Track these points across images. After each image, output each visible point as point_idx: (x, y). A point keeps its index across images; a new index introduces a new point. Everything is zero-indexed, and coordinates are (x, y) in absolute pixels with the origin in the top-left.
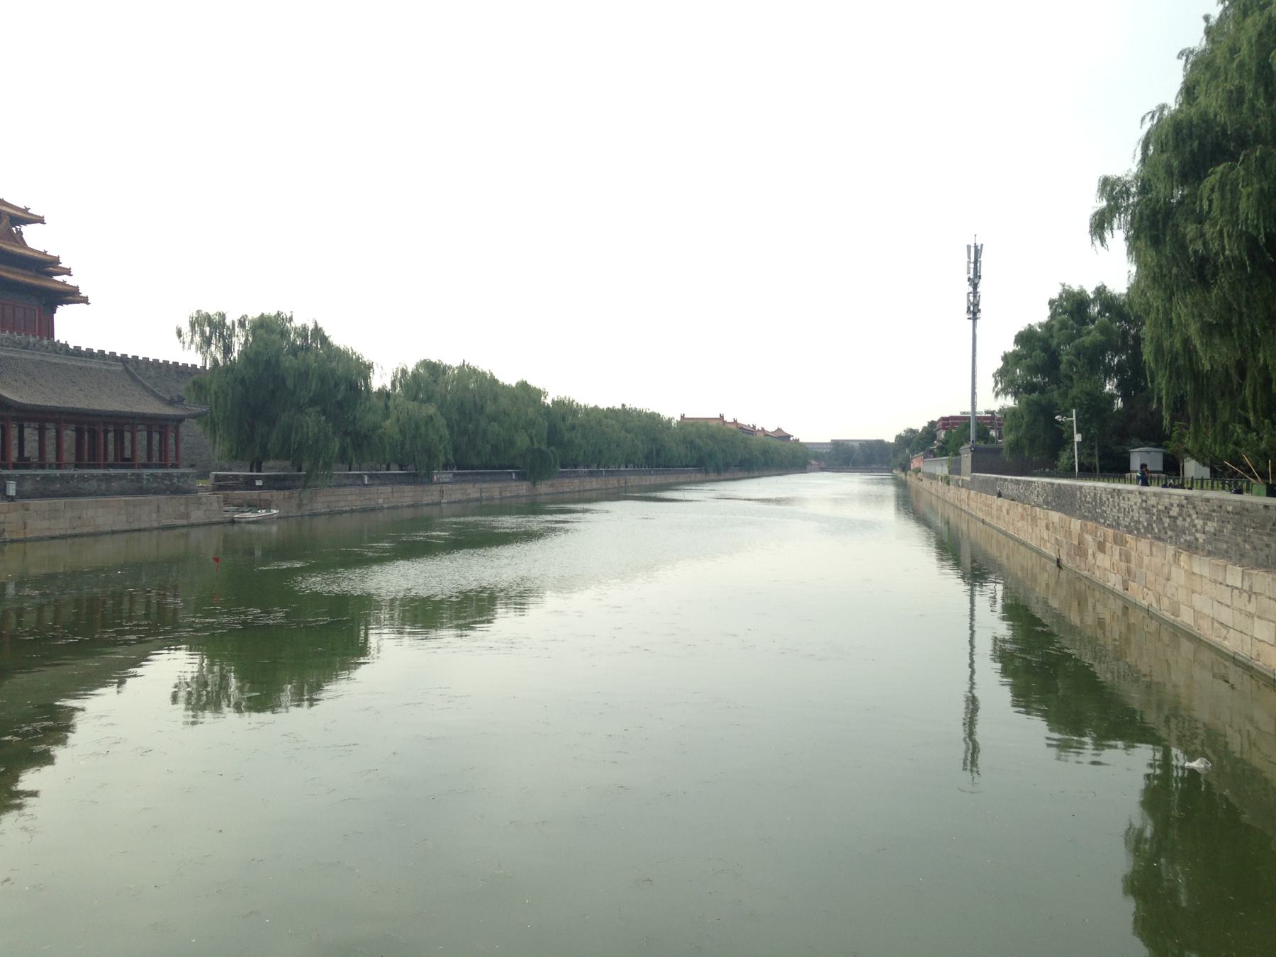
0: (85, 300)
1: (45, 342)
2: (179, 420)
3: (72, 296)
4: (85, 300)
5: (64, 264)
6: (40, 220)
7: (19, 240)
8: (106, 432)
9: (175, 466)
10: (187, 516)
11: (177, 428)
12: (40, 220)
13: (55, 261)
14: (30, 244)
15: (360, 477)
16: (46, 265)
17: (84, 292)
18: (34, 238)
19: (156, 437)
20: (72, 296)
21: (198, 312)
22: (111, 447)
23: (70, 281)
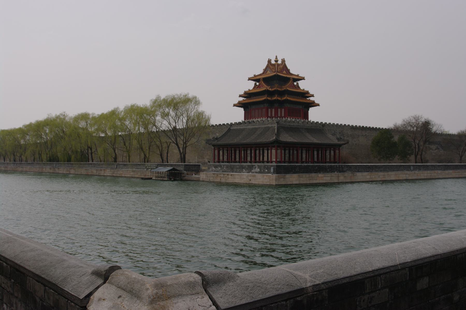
0: (318, 105)
1: (307, 121)
2: (340, 145)
3: (313, 104)
4: (318, 105)
5: (311, 93)
6: (303, 79)
7: (298, 87)
11: (339, 150)
12: (303, 79)
13: (308, 93)
14: (302, 88)
16: (305, 94)
17: (316, 102)
18: (303, 85)
19: (332, 152)
20: (313, 104)
22: (316, 156)
23: (312, 99)
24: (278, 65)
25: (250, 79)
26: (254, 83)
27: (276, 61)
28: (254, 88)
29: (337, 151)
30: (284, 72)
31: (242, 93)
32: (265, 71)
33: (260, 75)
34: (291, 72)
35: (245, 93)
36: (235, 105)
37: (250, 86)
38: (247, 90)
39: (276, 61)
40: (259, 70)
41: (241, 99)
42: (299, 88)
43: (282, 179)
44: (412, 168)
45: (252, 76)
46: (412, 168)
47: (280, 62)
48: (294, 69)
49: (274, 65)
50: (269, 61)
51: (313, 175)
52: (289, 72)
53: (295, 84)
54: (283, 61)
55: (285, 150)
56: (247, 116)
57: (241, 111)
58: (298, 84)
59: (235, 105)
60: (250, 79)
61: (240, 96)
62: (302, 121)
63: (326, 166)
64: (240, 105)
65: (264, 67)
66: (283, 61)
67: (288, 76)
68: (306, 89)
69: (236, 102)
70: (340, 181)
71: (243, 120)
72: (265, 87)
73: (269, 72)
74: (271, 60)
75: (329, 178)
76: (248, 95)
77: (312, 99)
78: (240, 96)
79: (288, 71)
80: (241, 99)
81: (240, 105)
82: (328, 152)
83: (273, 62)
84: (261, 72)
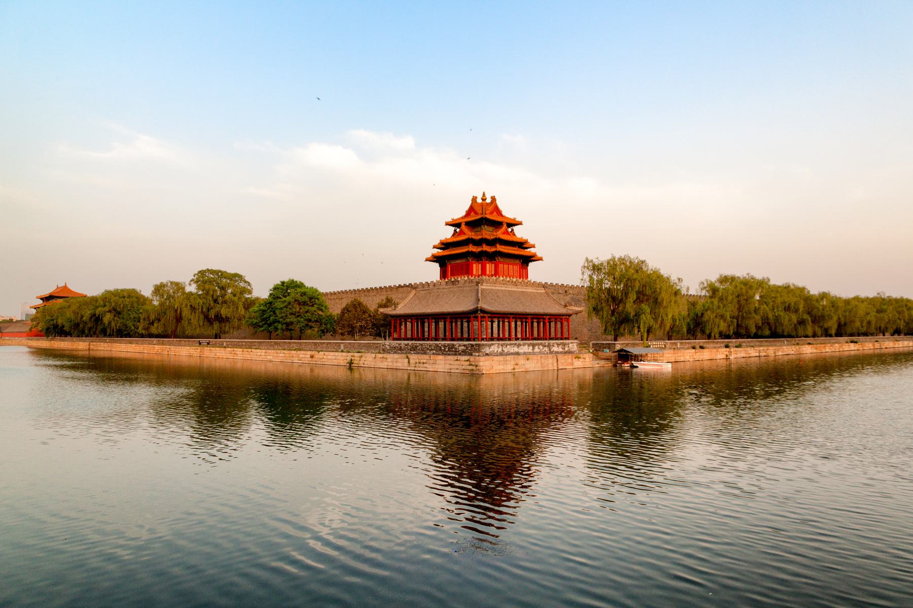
0: (541, 259)
2: (570, 315)
4: (541, 259)
5: (531, 241)
6: (520, 223)
8: (550, 323)
9: (568, 339)
10: (572, 364)
11: (568, 321)
12: (520, 223)
13: (526, 242)
15: (676, 344)
16: (522, 245)
17: (539, 255)
18: (520, 233)
21: (587, 259)
23: (532, 250)
24: (487, 204)
25: (447, 224)
26: (453, 228)
27: (484, 200)
28: (453, 235)
29: (565, 323)
31: (437, 242)
32: (468, 213)
33: (462, 218)
34: (504, 214)
35: (442, 243)
36: (427, 260)
37: (448, 233)
38: (443, 238)
39: (484, 200)
40: (459, 212)
41: (436, 251)
42: (514, 235)
45: (449, 220)
47: (489, 200)
48: (508, 211)
49: (482, 205)
50: (474, 199)
52: (502, 215)
53: (510, 230)
54: (493, 199)
55: (492, 322)
56: (443, 275)
57: (436, 266)
59: (427, 260)
60: (447, 224)
61: (435, 247)
64: (436, 259)
65: (467, 207)
66: (493, 199)
67: (499, 219)
68: (525, 238)
69: (429, 255)
71: (438, 279)
72: (469, 234)
73: (472, 214)
76: (445, 245)
77: (532, 250)
78: (435, 247)
79: (499, 213)
80: (436, 251)
81: (436, 259)
82: (553, 324)
83: (479, 201)
84: (464, 214)
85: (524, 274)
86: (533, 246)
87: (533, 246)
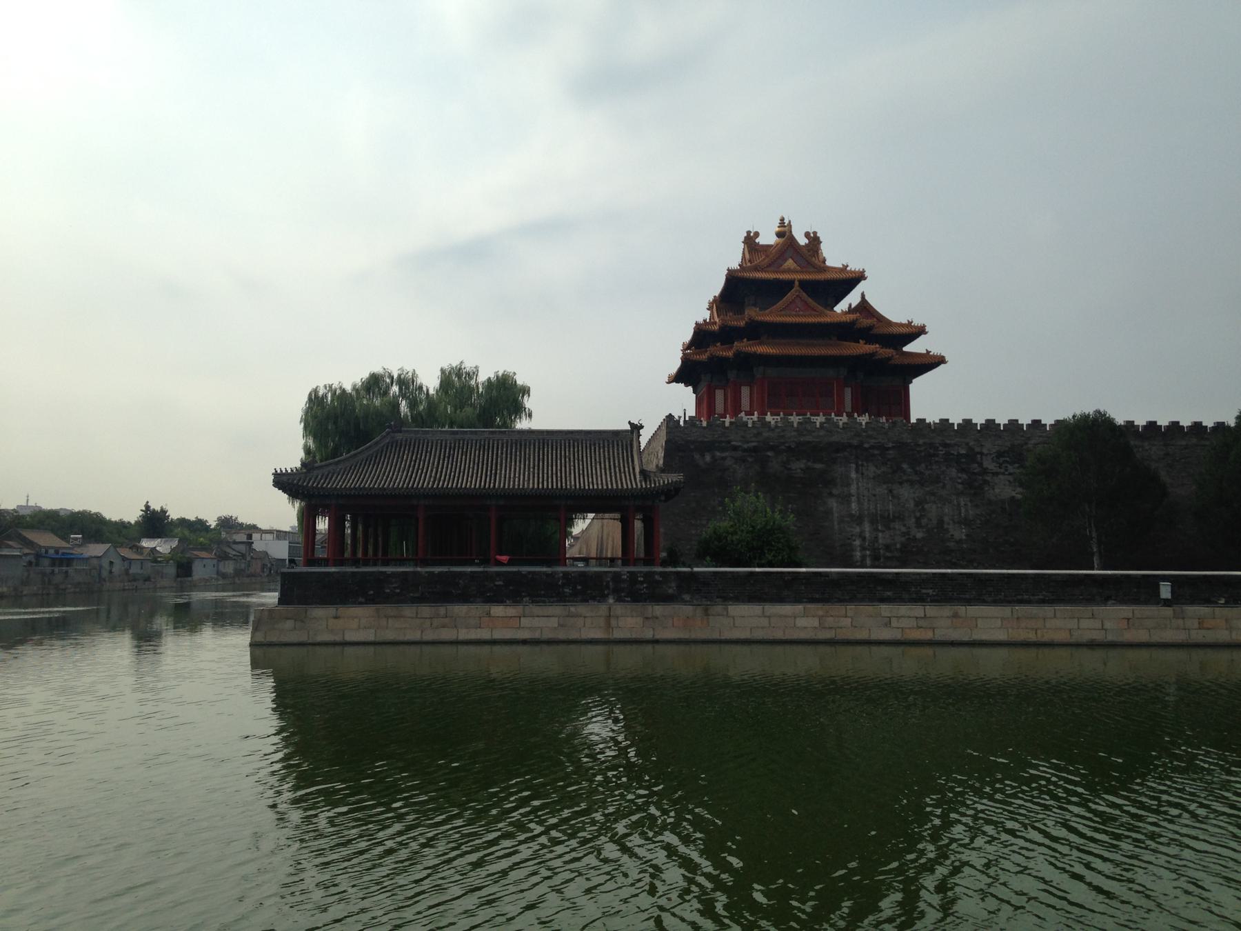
0: (940, 361)
4: (940, 361)
6: (859, 277)
7: (864, 307)
12: (859, 277)
30: (790, 263)
43: (289, 624)
44: (1165, 591)
46: (1165, 591)
51: (460, 610)
58: (863, 296)
62: (795, 419)
63: (552, 575)
70: (618, 635)
74: (757, 234)
75: (554, 622)
85: (902, 403)
86: (920, 331)
87: (920, 331)
